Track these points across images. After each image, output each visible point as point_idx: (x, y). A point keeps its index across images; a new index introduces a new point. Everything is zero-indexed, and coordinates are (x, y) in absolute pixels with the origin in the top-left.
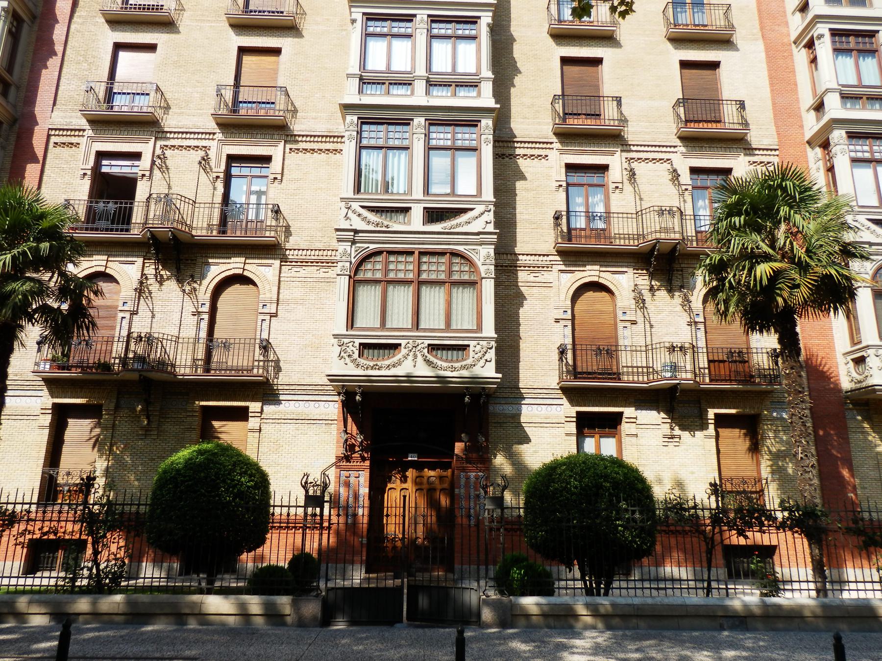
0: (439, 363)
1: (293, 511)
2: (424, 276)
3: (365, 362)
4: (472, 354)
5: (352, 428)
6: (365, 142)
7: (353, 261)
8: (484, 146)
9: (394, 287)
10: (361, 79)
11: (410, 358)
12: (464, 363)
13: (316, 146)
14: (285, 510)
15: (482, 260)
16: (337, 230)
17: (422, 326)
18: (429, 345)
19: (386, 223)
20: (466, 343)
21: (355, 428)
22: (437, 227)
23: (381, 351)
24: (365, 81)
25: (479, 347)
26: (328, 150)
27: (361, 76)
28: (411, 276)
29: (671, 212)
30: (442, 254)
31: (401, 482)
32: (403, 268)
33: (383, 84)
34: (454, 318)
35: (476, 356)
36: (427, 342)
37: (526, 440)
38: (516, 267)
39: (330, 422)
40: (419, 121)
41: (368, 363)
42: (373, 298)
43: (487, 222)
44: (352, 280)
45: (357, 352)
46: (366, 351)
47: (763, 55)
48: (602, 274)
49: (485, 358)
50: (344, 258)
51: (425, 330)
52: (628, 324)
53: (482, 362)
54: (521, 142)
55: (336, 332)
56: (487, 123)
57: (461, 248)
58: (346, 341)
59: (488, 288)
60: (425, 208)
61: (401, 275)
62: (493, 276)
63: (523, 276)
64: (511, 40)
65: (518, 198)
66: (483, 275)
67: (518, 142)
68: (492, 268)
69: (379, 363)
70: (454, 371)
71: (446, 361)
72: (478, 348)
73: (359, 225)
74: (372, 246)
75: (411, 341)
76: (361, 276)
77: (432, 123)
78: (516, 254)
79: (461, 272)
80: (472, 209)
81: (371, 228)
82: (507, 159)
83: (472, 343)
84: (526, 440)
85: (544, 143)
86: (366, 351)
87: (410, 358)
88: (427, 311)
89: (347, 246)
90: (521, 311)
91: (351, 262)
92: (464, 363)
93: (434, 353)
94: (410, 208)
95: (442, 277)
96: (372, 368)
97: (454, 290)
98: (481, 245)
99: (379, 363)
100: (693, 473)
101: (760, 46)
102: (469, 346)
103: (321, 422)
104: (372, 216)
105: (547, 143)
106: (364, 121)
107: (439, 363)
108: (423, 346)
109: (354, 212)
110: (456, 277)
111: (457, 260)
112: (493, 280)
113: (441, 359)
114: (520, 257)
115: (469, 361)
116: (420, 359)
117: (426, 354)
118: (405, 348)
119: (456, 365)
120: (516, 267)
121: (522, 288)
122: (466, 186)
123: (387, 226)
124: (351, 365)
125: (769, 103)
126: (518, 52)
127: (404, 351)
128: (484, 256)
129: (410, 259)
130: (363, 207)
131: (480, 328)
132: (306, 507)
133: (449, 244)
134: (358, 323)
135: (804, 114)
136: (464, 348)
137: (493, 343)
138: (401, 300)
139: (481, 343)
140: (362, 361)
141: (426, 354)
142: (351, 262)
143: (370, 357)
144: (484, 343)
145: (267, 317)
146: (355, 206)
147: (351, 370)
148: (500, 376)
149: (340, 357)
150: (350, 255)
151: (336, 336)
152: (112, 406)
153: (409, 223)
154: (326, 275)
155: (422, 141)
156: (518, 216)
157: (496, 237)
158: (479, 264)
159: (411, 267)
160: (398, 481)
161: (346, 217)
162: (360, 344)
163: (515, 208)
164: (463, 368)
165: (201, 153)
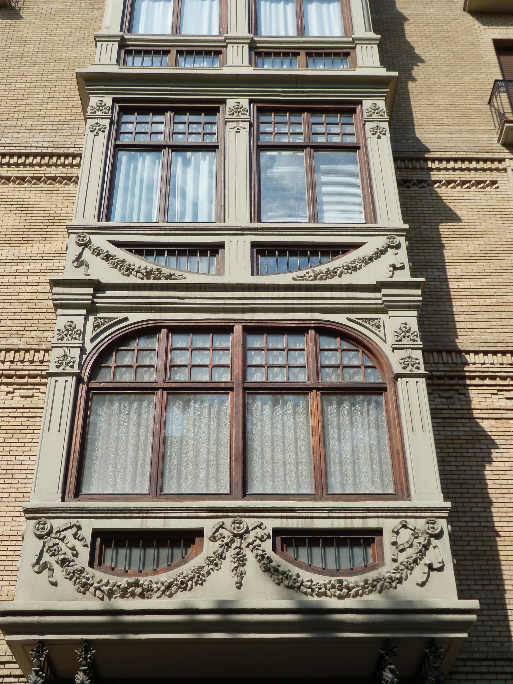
0: (305, 576)
2: (257, 377)
3: (106, 578)
4: (389, 551)
6: (126, 140)
7: (89, 346)
8: (372, 142)
9: (186, 404)
10: (123, 44)
11: (227, 564)
12: (371, 575)
13: (28, 172)
15: (391, 339)
16: (55, 283)
17: (255, 488)
18: (276, 532)
19: (166, 271)
20: (372, 523)
23: (150, 552)
24: (127, 49)
25: (405, 535)
26: (54, 179)
27: (122, 38)
28: (224, 377)
32: (209, 360)
33: (166, 53)
34: (334, 469)
35: (402, 557)
36: (271, 524)
38: (464, 378)
40: (237, 103)
41: (113, 579)
42: (133, 428)
43: (394, 266)
44: (83, 388)
45: (85, 553)
46: (109, 553)
49: (427, 560)
50: (66, 340)
53: (419, 573)
54: (440, 160)
55: (34, 503)
56: (373, 105)
57: (340, 318)
58: (58, 524)
59: (414, 398)
60: (254, 245)
61: (202, 377)
62: (422, 370)
63: (480, 398)
64: (402, 19)
65: (447, 253)
66: (398, 369)
67: (433, 160)
68: (418, 355)
69: (144, 580)
70: (342, 592)
71: (324, 571)
72: (405, 535)
74: (134, 318)
75: (228, 522)
76: (105, 379)
77: (263, 109)
78: (459, 352)
80: (356, 246)
81: (132, 279)
82: (415, 188)
83: (388, 525)
85: (485, 160)
86: (109, 553)
87: (227, 564)
88: (268, 456)
89: (77, 316)
90: (488, 471)
91: (83, 350)
92: (371, 575)
93: (291, 552)
94: (222, 245)
95: (301, 377)
96: (124, 593)
97: (332, 409)
98: (385, 310)
99: (144, 580)
102: (379, 532)
105: (492, 160)
106: (126, 108)
107: (305, 576)
108: (259, 532)
109: (97, 252)
111: (335, 343)
112: (423, 382)
113: (310, 568)
114: (471, 358)
115: (387, 569)
116: (252, 565)
117: (269, 552)
118: (213, 539)
119: (351, 580)
120: (464, 378)
121: (483, 424)
122: (340, 210)
123: (170, 276)
124: (67, 586)
126: (412, 33)
127: (209, 548)
128: (395, 333)
129: (222, 341)
131: (403, 490)
133: (312, 310)
134: (94, 485)
136: (368, 537)
137: (442, 524)
138: (200, 432)
139: (411, 523)
140: (98, 575)
141: (269, 552)
142: (83, 350)
143: (121, 567)
144: (420, 524)
147: (67, 598)
148: (474, 604)
149: (40, 565)
150: (83, 334)
153: (220, 272)
154: (28, 402)
155: (244, 135)
156: (453, 285)
157: (419, 292)
158: (386, 348)
159: (226, 360)
161: (79, 262)
162: (96, 533)
163: (443, 270)
164: (371, 587)
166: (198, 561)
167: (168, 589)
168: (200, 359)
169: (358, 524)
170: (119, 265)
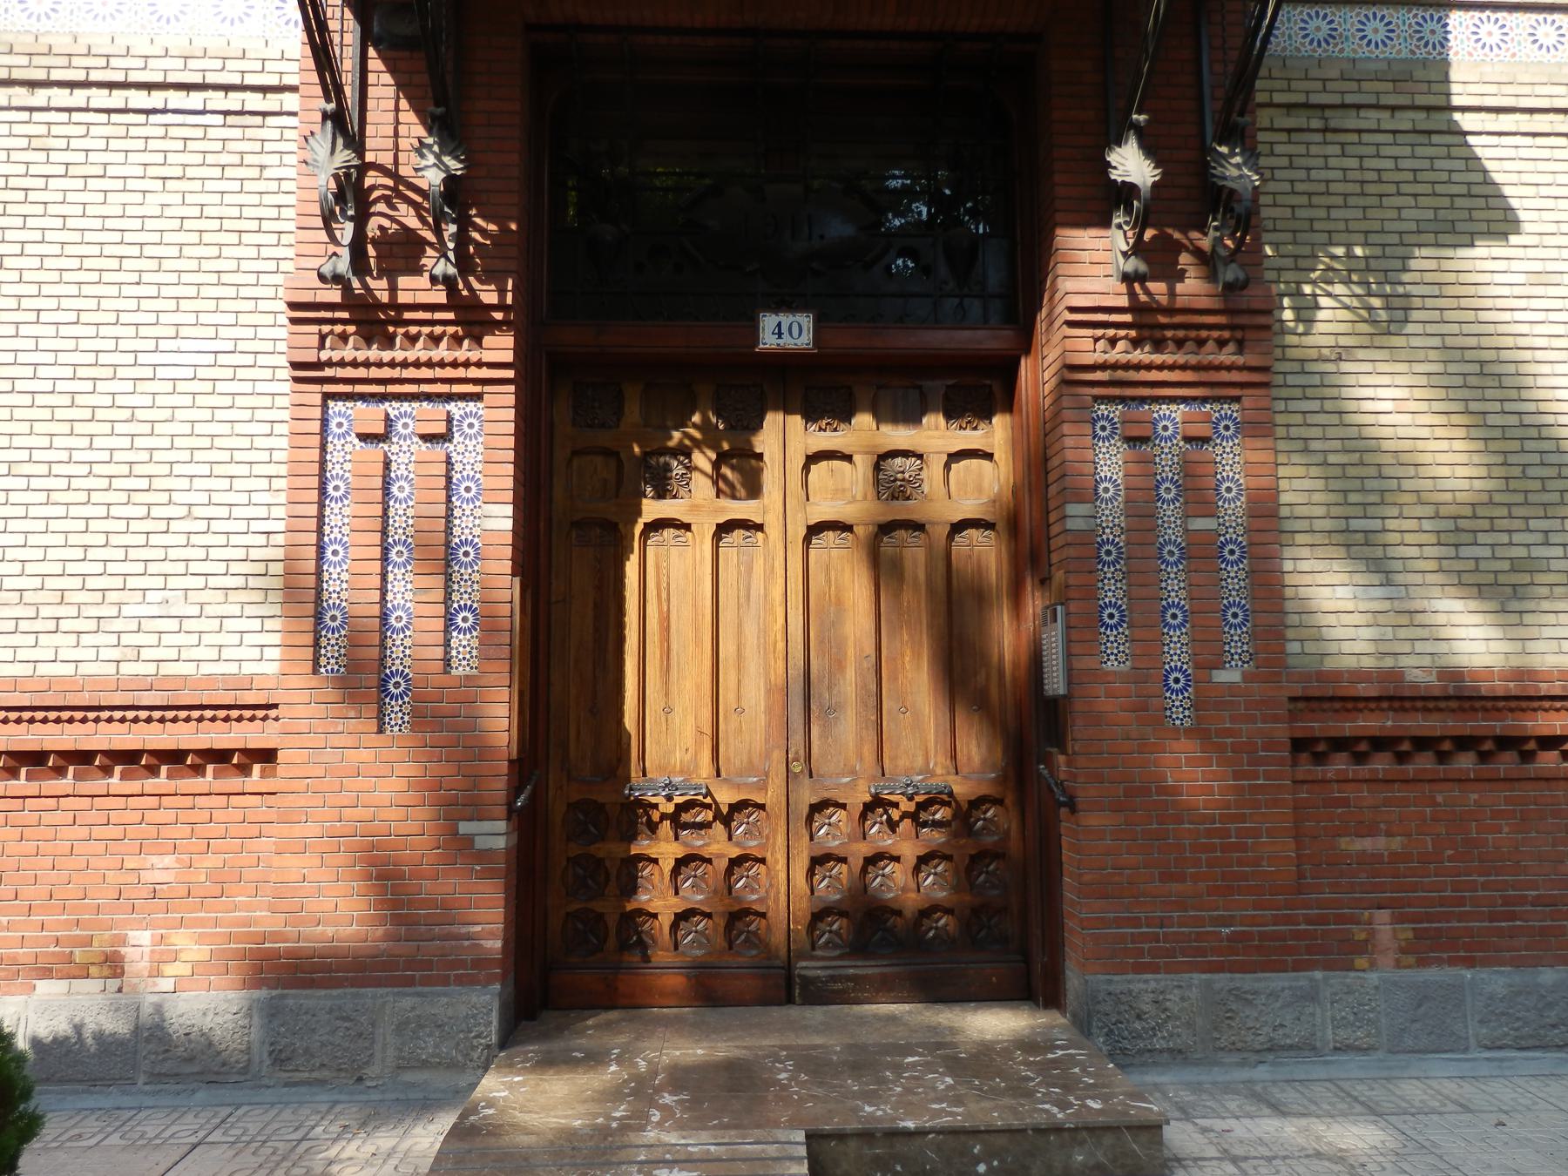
5: (396, 129)
21: (412, 128)
31: (723, 488)
37: (1487, 215)
39: (254, 101)
84: (1487, 215)
103: (195, 100)
160: (701, 486)
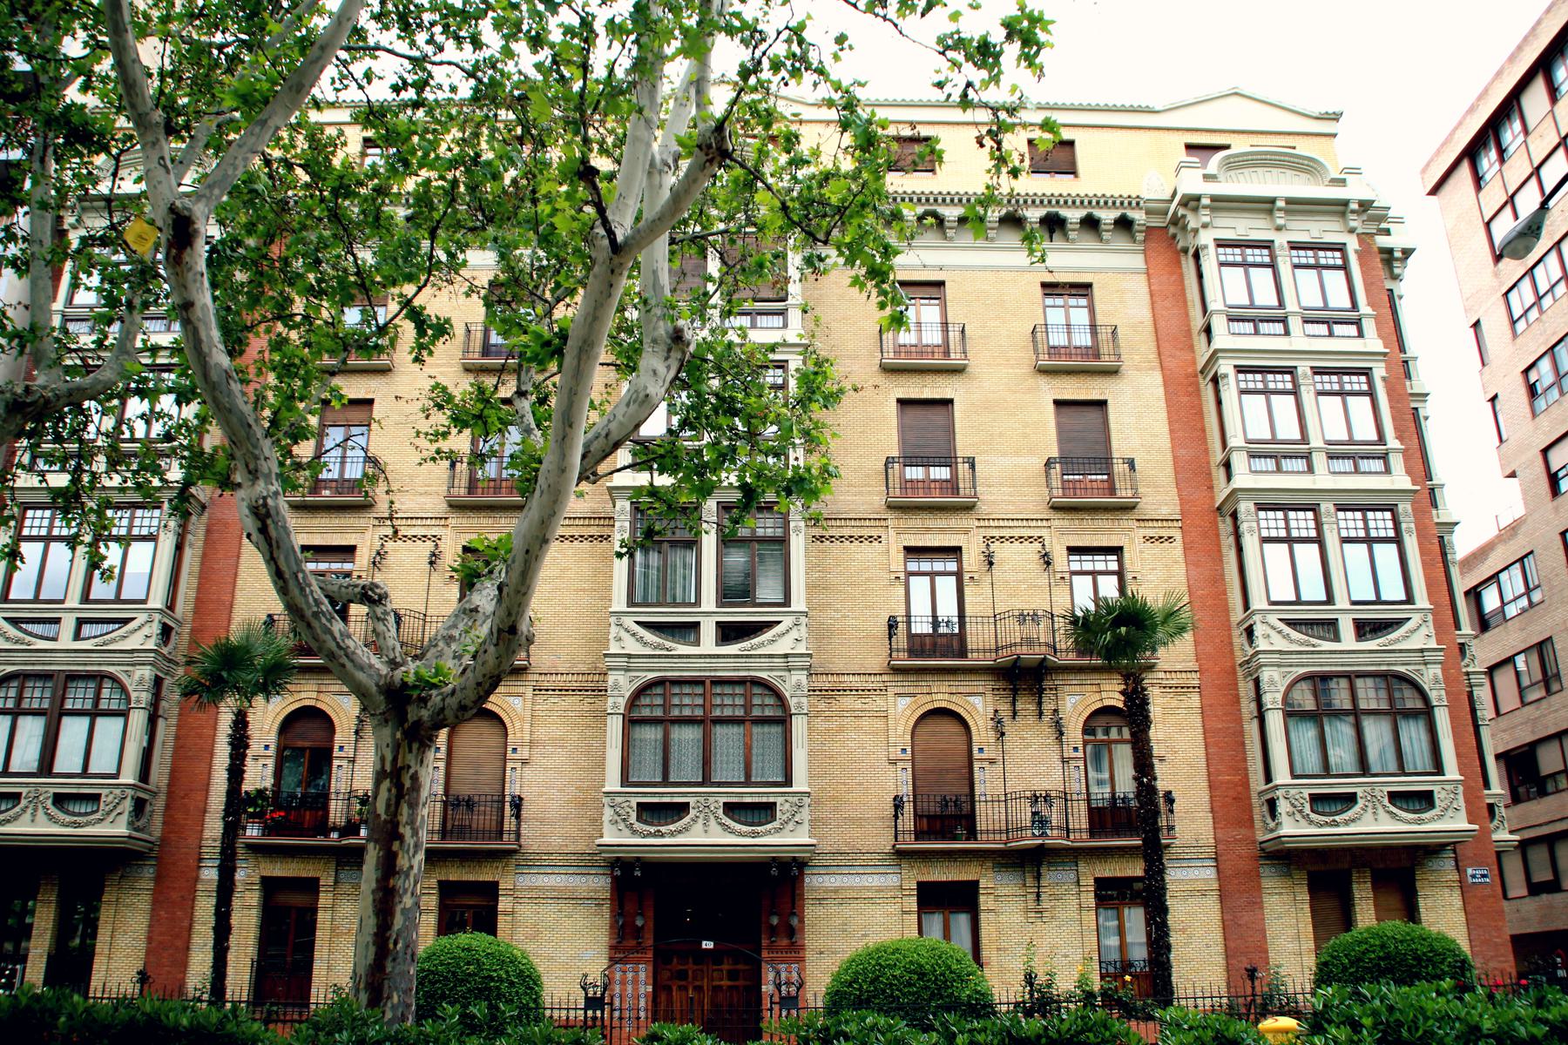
1: (572, 1014)
12: (769, 826)
14: (564, 1013)
20: (771, 800)
22: (733, 649)
29: (1035, 617)
30: (741, 682)
45: (634, 815)
47: (1161, 390)
48: (954, 698)
51: (719, 784)
52: (985, 764)
53: (791, 826)
57: (764, 675)
73: (633, 647)
74: (651, 675)
76: (635, 714)
79: (763, 705)
83: (779, 800)
100: (1066, 956)
101: (1157, 378)
104: (649, 636)
107: (738, 827)
109: (627, 630)
110: (756, 712)
124: (627, 832)
125: (1169, 456)
130: (638, 623)
132: (586, 1010)
135: (1214, 471)
140: (638, 826)
145: (518, 765)
146: (629, 622)
151: (608, 794)
152: (331, 881)
153: (697, 643)
165: (430, 545)
166: (687, 820)
167: (672, 834)
168: (687, 701)
169: (764, 800)
170: (641, 640)
